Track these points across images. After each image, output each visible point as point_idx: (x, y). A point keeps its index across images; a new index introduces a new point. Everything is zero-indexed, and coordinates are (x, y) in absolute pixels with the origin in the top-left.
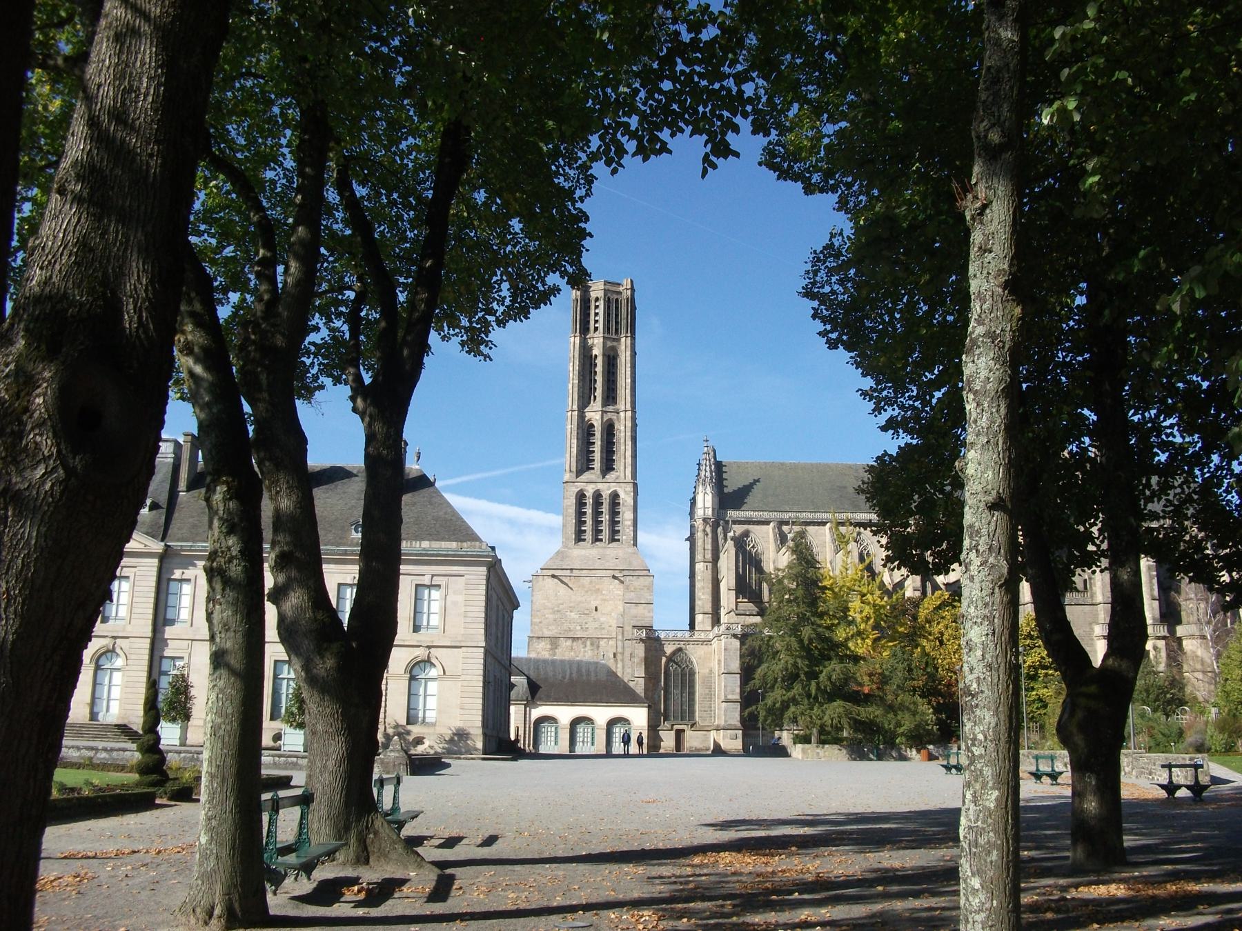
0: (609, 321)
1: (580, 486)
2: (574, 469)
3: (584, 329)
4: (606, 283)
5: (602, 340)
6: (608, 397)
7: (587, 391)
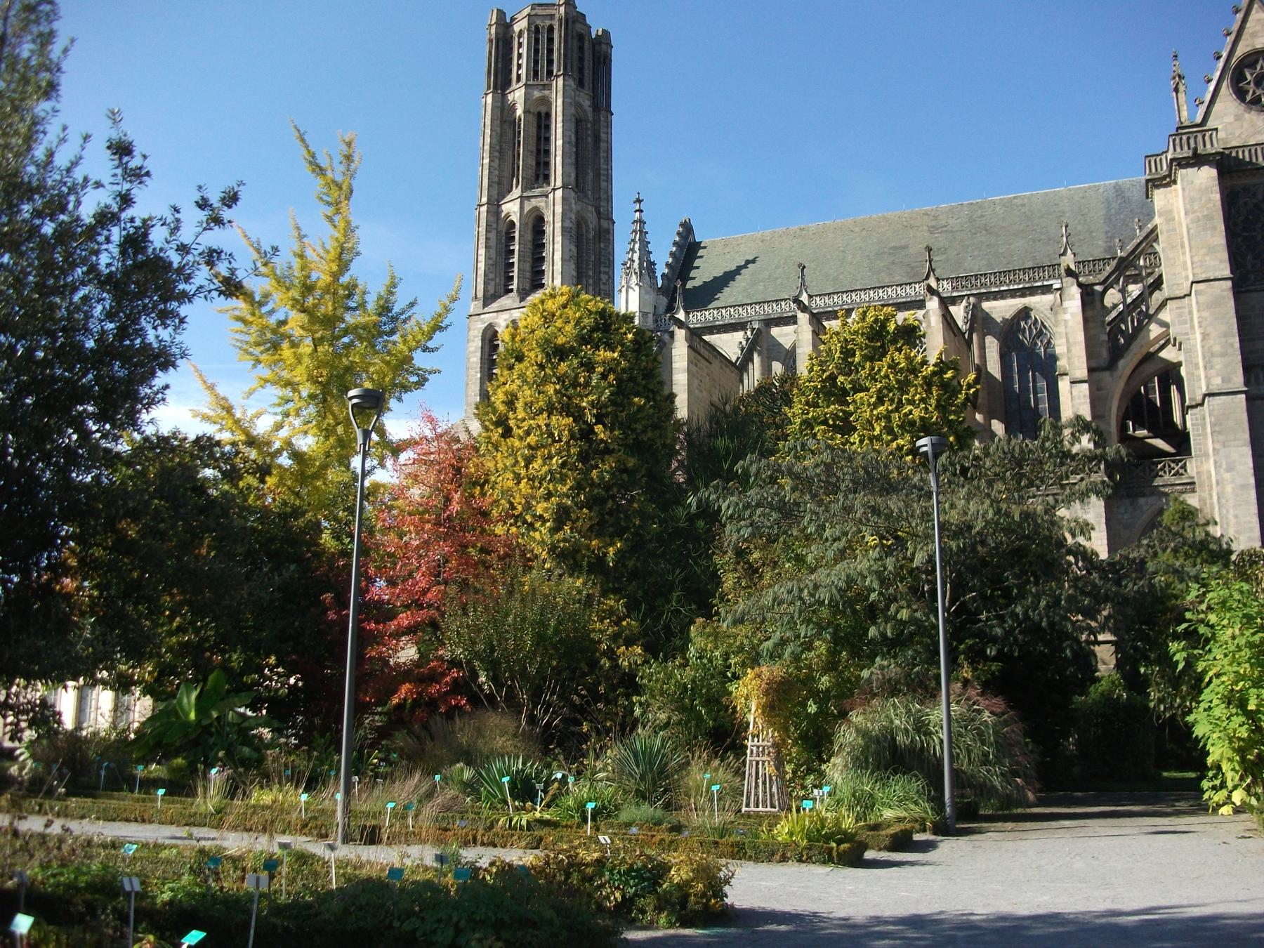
0: (536, 62)
1: (488, 318)
2: (480, 294)
3: (501, 79)
4: (533, 7)
5: (523, 90)
6: (537, 177)
7: (507, 174)
